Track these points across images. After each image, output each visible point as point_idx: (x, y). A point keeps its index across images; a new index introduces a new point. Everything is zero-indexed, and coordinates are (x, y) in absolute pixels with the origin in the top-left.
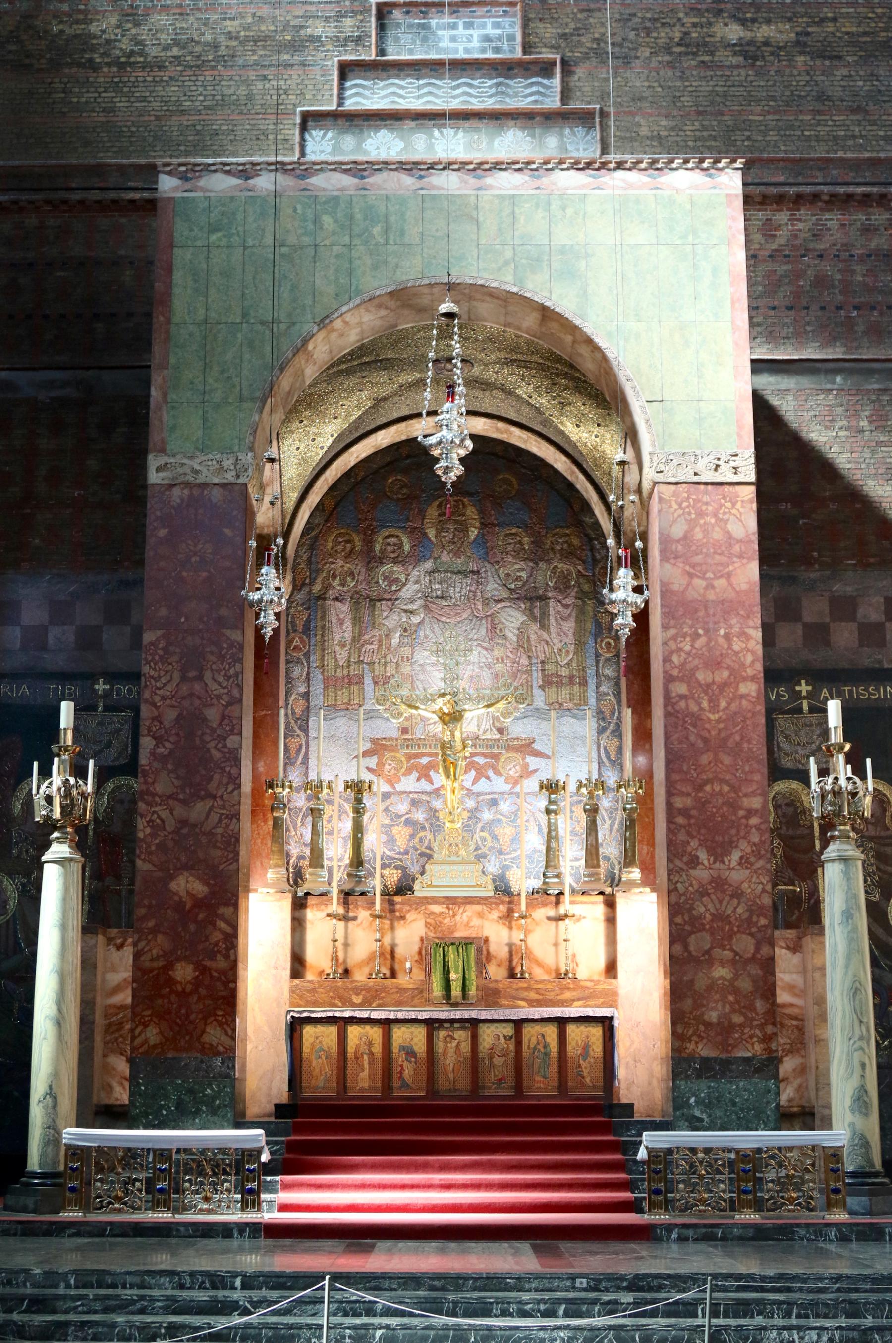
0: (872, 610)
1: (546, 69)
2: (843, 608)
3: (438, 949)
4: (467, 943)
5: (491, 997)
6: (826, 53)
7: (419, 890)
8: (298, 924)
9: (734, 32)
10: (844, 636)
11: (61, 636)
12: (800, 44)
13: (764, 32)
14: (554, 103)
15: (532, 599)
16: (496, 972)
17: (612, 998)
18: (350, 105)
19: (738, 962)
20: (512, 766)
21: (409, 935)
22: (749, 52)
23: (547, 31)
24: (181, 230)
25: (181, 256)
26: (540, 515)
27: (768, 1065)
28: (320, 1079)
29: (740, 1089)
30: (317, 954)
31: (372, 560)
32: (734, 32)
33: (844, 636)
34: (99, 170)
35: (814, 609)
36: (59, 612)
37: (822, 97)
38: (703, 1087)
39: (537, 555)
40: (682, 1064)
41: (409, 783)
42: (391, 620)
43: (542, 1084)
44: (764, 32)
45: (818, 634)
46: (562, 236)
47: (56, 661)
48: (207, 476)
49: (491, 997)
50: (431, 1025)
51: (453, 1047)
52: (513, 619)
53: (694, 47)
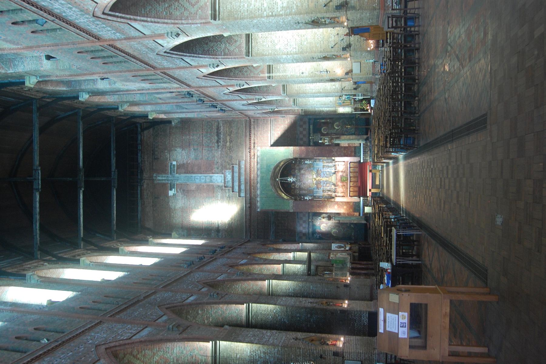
0: (301, 129)
1: (233, 167)
2: (301, 133)
3: (342, 181)
4: (341, 178)
5: (347, 175)
6: (231, 132)
7: (335, 183)
8: (339, 196)
9: (228, 144)
10: (305, 133)
11: (304, 225)
12: (230, 135)
13: (228, 140)
14: (237, 166)
15: (300, 169)
16: (344, 175)
17: (348, 162)
18: (237, 191)
19: (344, 150)
20: (320, 172)
21: (340, 184)
22: (231, 142)
23: (228, 166)
24: (264, 208)
25: (267, 208)
26: (288, 168)
27: (355, 147)
28: (357, 194)
29: (357, 150)
30: (342, 195)
31: (295, 188)
32: (228, 144)
33: (305, 133)
34: (246, 222)
35: (301, 136)
36: (301, 225)
37: (237, 133)
38: (357, 154)
39: (295, 169)
40: (355, 156)
41: (322, 184)
42: (302, 186)
43: (357, 170)
44: (228, 140)
45: (304, 136)
46: (265, 167)
47: (307, 226)
48: (292, 205)
49: (347, 175)
50: (350, 182)
51: (353, 179)
52: (302, 172)
53: (230, 148)
